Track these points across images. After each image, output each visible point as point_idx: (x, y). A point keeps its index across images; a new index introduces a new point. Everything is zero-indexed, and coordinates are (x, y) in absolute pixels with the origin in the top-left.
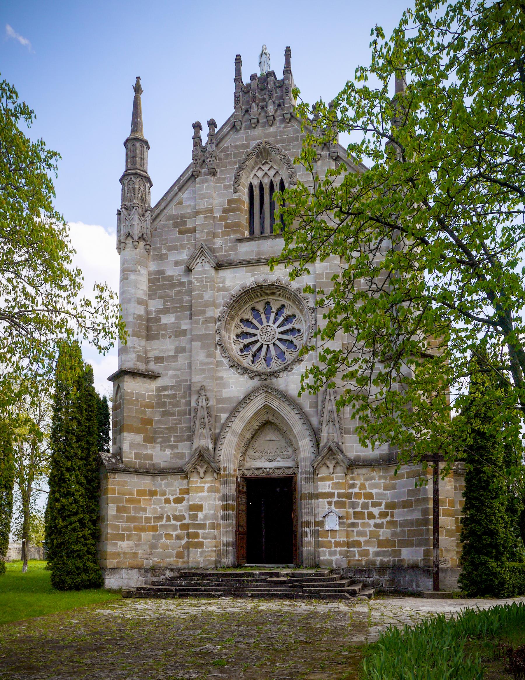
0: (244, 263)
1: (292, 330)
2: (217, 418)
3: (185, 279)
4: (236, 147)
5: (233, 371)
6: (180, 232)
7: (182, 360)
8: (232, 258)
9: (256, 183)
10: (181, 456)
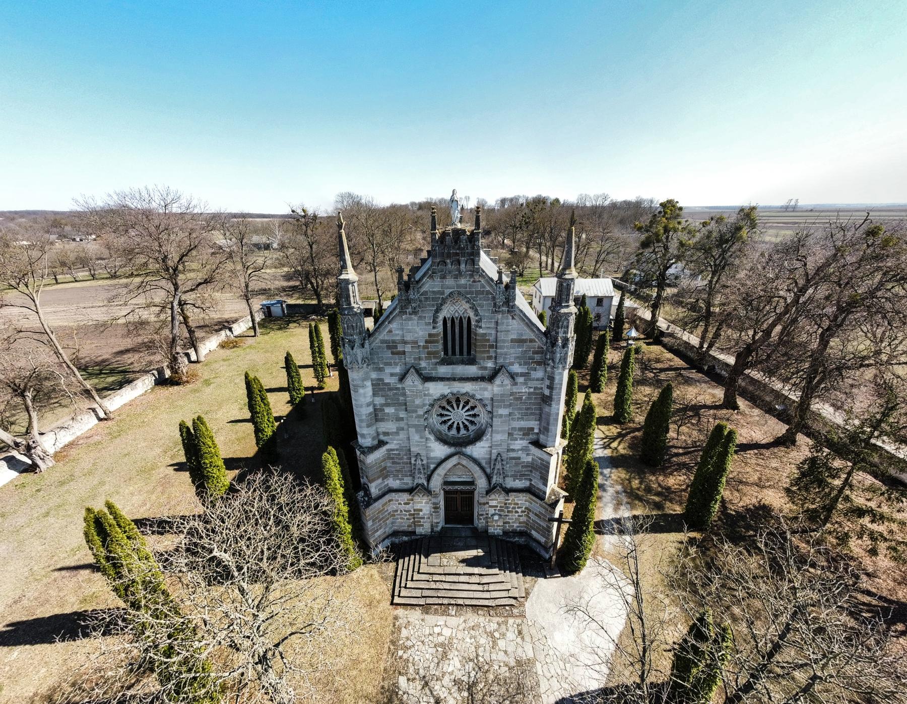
0: (442, 379)
1: (475, 416)
2: (428, 467)
3: (399, 386)
4: (433, 292)
5: (437, 443)
6: (393, 353)
7: (402, 435)
8: (434, 375)
10: (407, 484)
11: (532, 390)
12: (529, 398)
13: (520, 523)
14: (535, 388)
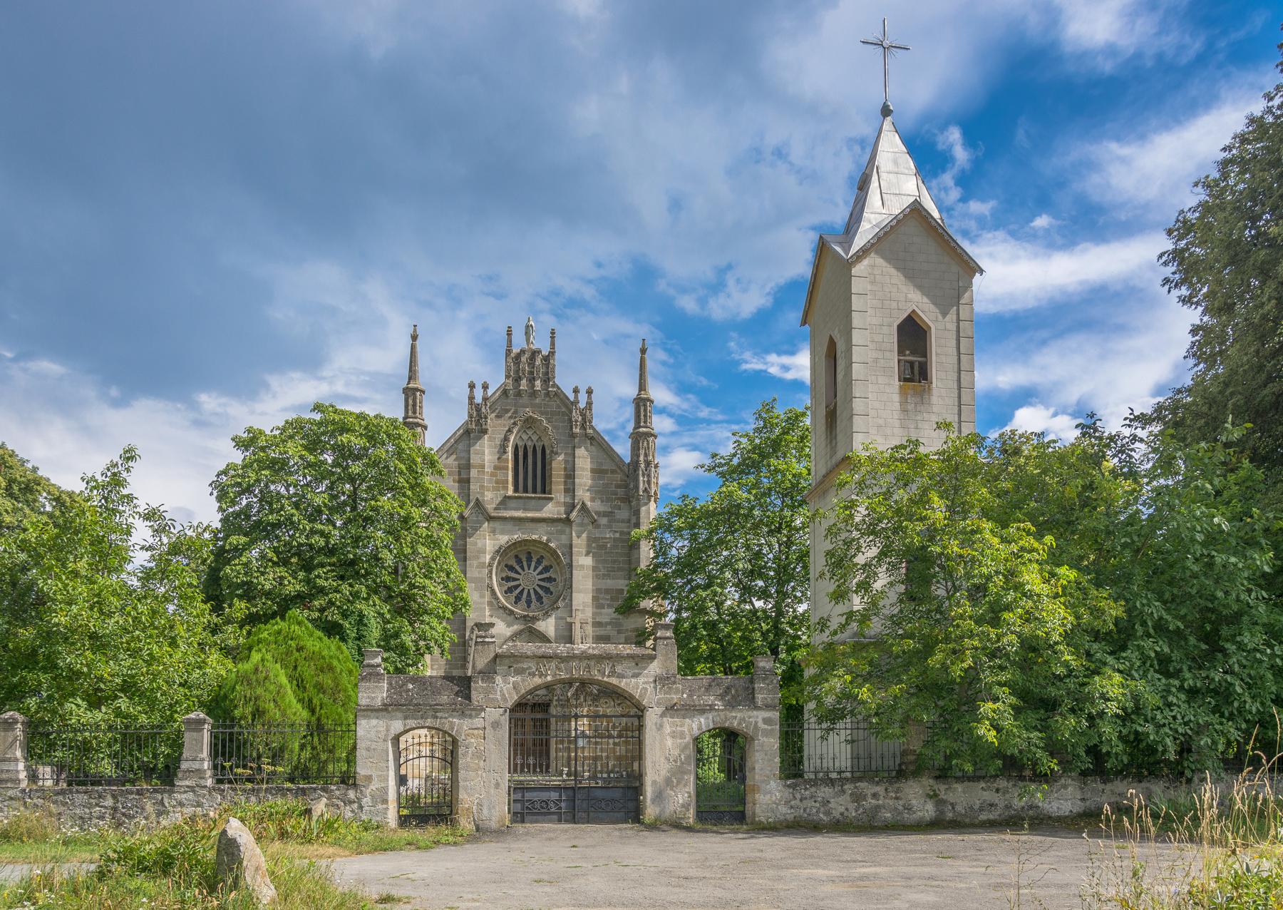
9: (520, 444)
11: (617, 535)
12: (614, 547)
14: (622, 533)
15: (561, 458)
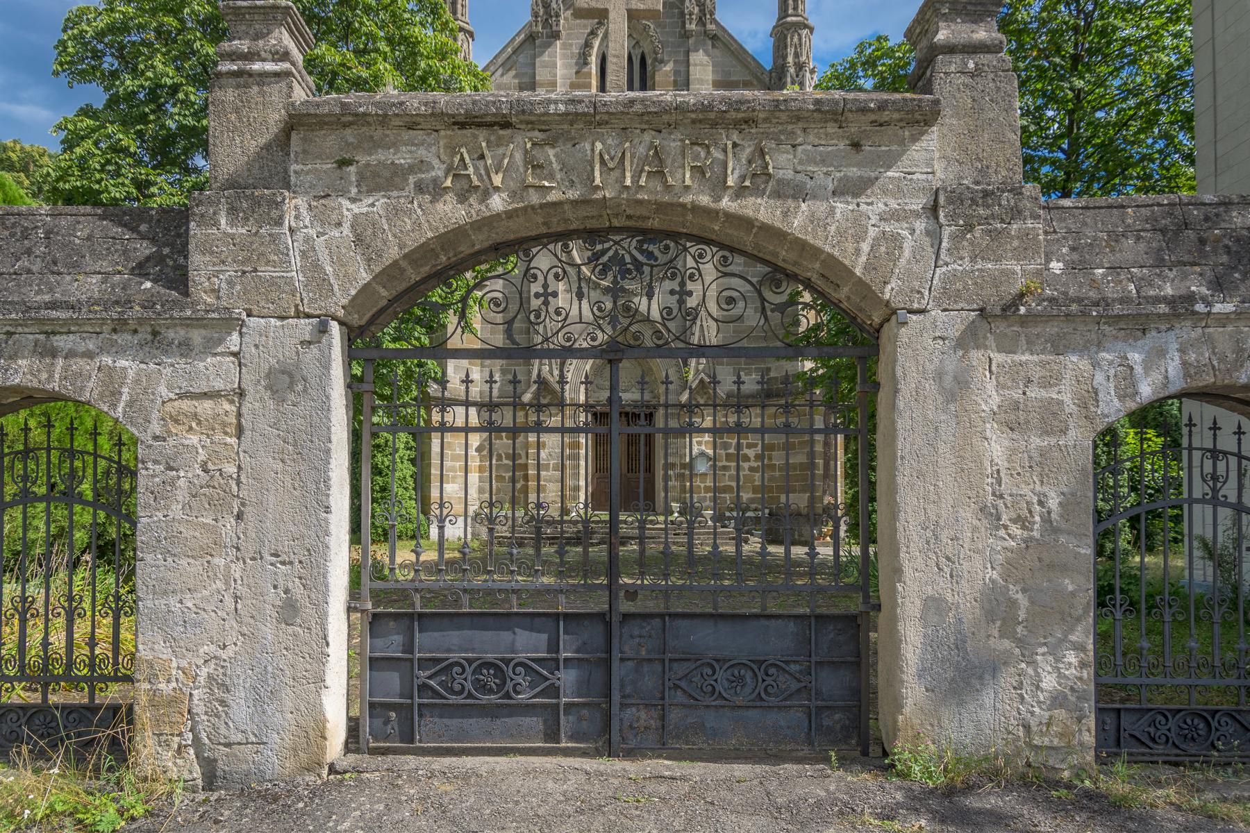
13: (755, 490)
15: (669, 67)
